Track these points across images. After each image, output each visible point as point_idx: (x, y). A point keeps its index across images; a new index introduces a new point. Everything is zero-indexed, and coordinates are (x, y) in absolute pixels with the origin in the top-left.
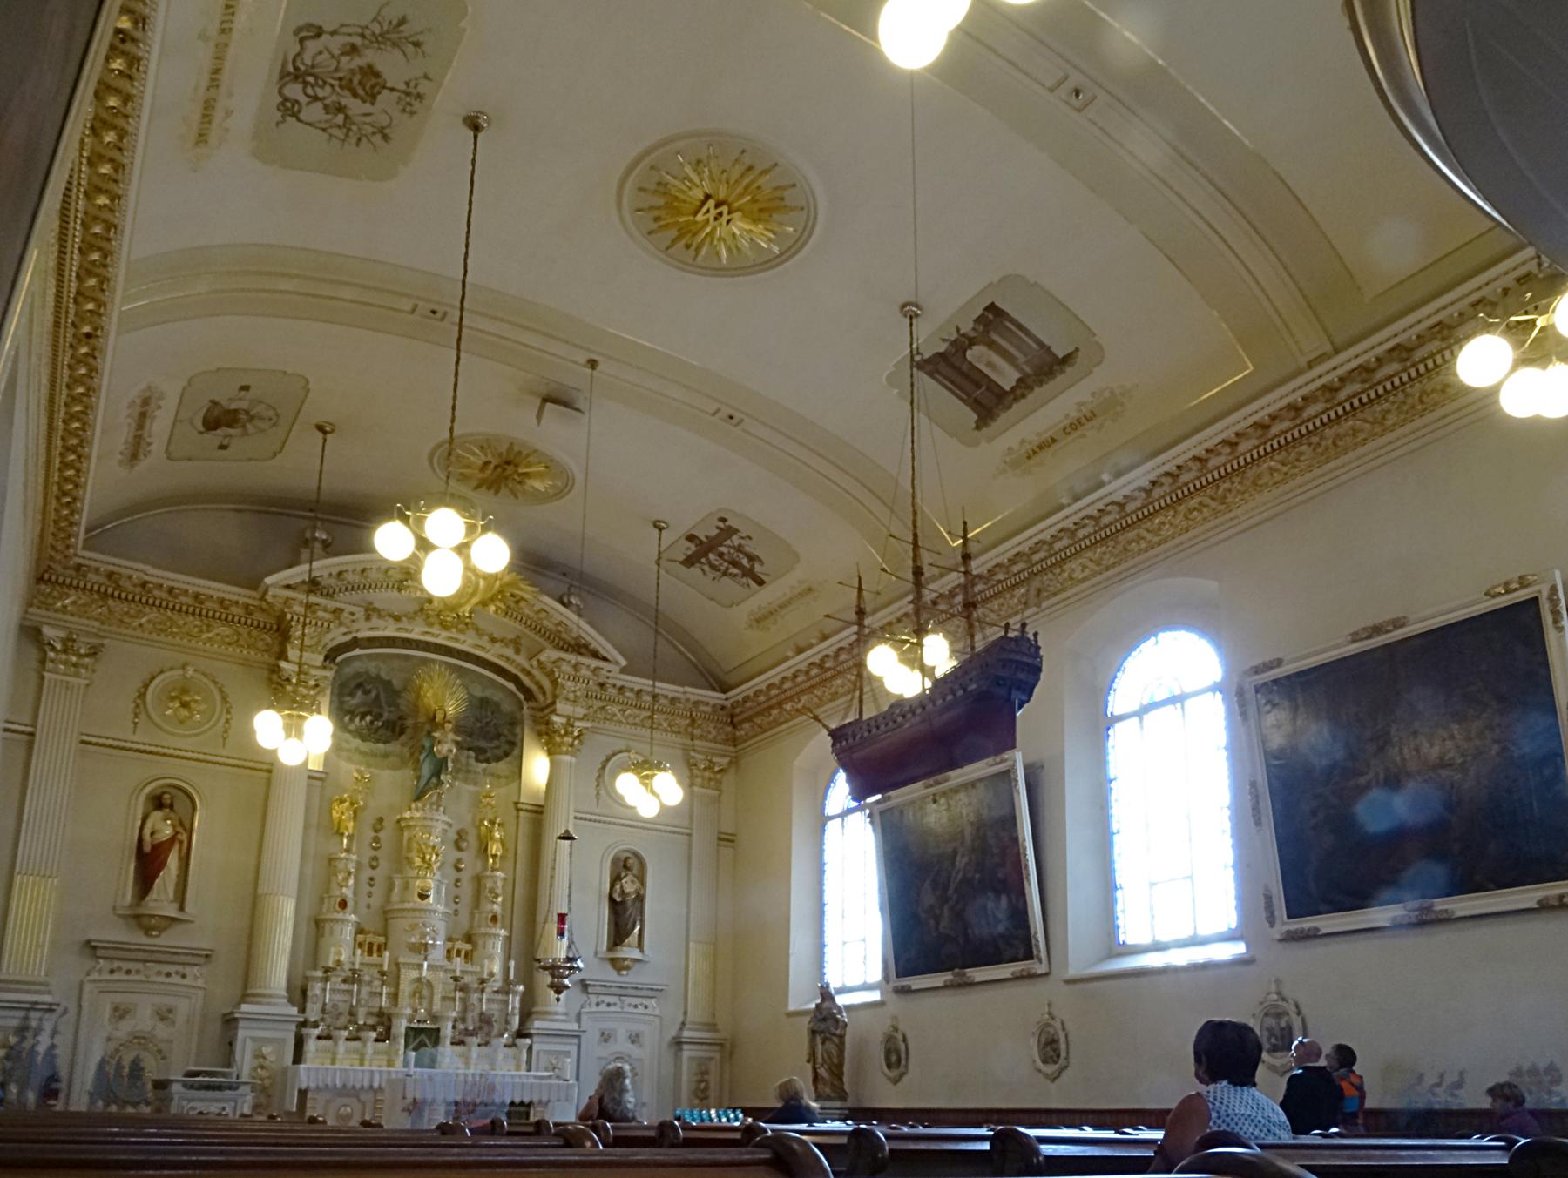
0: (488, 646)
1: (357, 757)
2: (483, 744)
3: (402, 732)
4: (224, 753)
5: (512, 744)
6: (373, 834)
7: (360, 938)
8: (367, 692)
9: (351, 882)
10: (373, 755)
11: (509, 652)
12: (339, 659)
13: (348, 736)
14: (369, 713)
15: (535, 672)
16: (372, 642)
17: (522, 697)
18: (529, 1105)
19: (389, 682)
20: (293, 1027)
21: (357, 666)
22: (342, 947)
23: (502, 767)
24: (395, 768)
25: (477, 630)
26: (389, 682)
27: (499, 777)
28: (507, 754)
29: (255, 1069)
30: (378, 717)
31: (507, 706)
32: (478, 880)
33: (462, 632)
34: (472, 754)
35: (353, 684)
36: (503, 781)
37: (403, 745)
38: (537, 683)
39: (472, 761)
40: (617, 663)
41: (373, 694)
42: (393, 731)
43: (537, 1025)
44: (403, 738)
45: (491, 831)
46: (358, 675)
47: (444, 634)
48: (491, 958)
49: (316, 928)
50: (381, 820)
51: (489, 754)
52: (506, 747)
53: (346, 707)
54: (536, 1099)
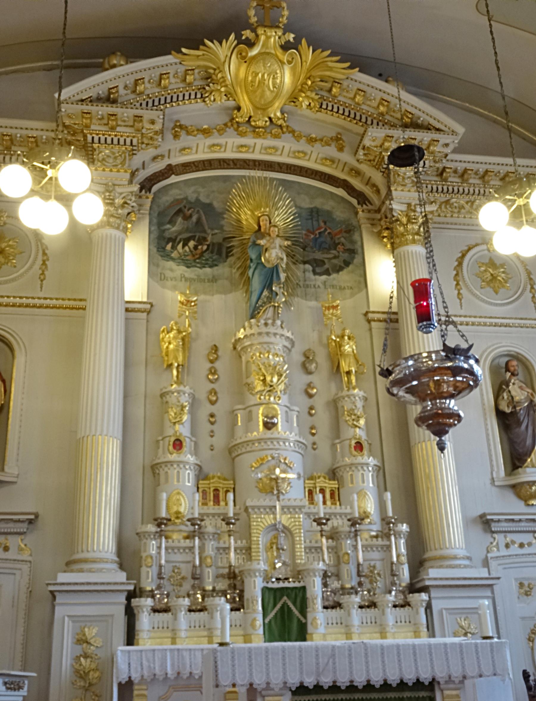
0: (307, 148)
1: (182, 284)
2: (319, 255)
3: (229, 252)
4: (41, 295)
5: (352, 252)
6: (209, 365)
7: (203, 484)
8: (187, 218)
9: (185, 418)
10: (200, 280)
11: (332, 151)
12: (155, 188)
14: (192, 238)
15: (364, 168)
16: (187, 167)
17: (354, 201)
18: (433, 684)
19: (210, 205)
20: (122, 599)
21: (175, 194)
22: (182, 496)
23: (344, 277)
24: (225, 292)
25: (293, 132)
26: (210, 205)
27: (342, 289)
28: (347, 264)
29: (78, 658)
30: (201, 241)
31: (340, 214)
32: (335, 405)
33: (276, 136)
34: (308, 266)
35: (173, 211)
37: (231, 267)
38: (368, 182)
39: (310, 275)
41: (194, 218)
42: (219, 253)
43: (433, 574)
44: (231, 260)
45: (340, 346)
46: (178, 201)
47: (260, 142)
48: (361, 494)
49: (146, 477)
50: (215, 348)
51: (327, 266)
52: (345, 256)
53: (167, 235)
54: (441, 675)
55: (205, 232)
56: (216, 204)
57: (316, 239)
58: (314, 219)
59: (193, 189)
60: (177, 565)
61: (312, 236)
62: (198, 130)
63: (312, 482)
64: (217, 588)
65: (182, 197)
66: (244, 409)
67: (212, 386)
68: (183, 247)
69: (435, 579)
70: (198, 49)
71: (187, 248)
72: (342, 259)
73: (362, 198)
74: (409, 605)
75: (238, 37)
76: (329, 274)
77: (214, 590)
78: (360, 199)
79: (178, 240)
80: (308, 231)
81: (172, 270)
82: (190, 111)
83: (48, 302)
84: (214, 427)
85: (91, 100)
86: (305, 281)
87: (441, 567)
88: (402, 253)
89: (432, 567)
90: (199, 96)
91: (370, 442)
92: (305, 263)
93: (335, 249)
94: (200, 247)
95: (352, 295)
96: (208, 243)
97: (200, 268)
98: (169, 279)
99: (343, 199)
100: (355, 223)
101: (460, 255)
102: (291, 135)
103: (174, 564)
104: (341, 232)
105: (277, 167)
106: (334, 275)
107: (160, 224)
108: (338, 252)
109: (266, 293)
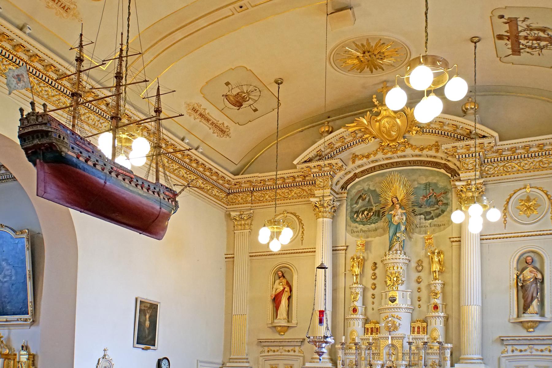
2: (428, 209)
8: (363, 200)
13: (356, 224)
14: (366, 210)
21: (359, 187)
28: (443, 211)
31: (442, 184)
34: (422, 216)
39: (423, 221)
41: (367, 200)
42: (379, 216)
46: (359, 191)
50: (375, 264)
51: (432, 215)
52: (443, 207)
53: (354, 210)
55: (372, 205)
56: (377, 190)
57: (427, 200)
59: (366, 184)
67: (374, 281)
71: (363, 215)
72: (441, 209)
80: (424, 196)
81: (356, 228)
85: (310, 160)
92: (421, 214)
100: (449, 188)
105: (408, 164)
106: (436, 219)
107: (351, 205)
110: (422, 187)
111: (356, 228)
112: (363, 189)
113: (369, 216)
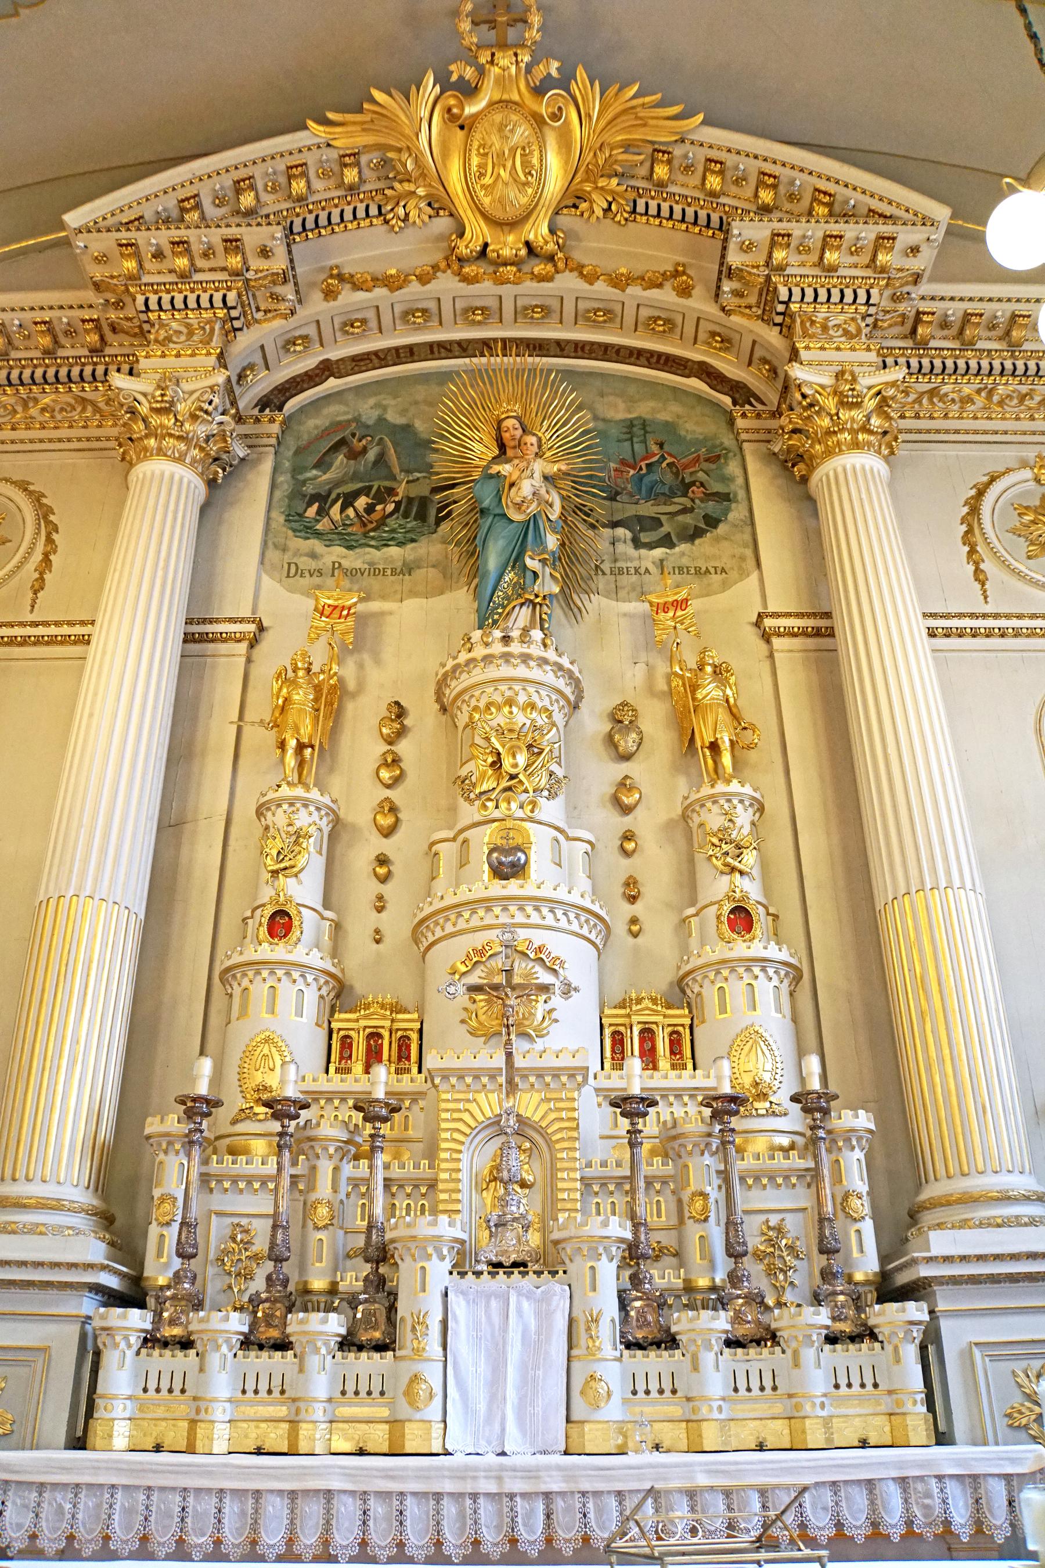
2: (647, 509)
8: (354, 455)
12: (292, 404)
13: (315, 544)
14: (366, 491)
17: (727, 400)
19: (407, 428)
21: (335, 412)
26: (407, 428)
28: (712, 522)
31: (697, 427)
34: (621, 531)
36: (716, 578)
37: (445, 542)
39: (627, 549)
40: (926, 221)
41: (371, 455)
42: (422, 516)
50: (399, 711)
51: (666, 528)
53: (309, 489)
56: (419, 425)
58: (635, 440)
59: (372, 401)
60: (244, 1222)
61: (632, 472)
62: (375, 279)
63: (622, 1012)
64: (342, 1286)
65: (350, 417)
66: (454, 839)
67: (388, 793)
68: (343, 509)
69: (947, 1259)
70: (360, 110)
71: (351, 512)
72: (700, 512)
73: (740, 393)
74: (873, 1336)
75: (444, 82)
76: (671, 545)
77: (333, 1290)
78: (737, 396)
79: (333, 496)
81: (313, 555)
82: (364, 248)
83: (41, 631)
84: (386, 890)
86: (615, 561)
87: (964, 1224)
88: (831, 474)
89: (940, 1226)
90: (373, 211)
91: (772, 910)
92: (614, 525)
93: (685, 495)
94: (379, 508)
95: (725, 586)
96: (397, 499)
97: (377, 548)
98: (307, 574)
99: (700, 399)
100: (728, 441)
101: (973, 492)
102: (576, 274)
103: (236, 1220)
104: (697, 460)
105: (554, 349)
106: (683, 547)
107: (296, 470)
108: (693, 500)
109: (509, 576)
110: (614, 432)
111: (313, 555)
112: (357, 420)
113: (375, 516)
